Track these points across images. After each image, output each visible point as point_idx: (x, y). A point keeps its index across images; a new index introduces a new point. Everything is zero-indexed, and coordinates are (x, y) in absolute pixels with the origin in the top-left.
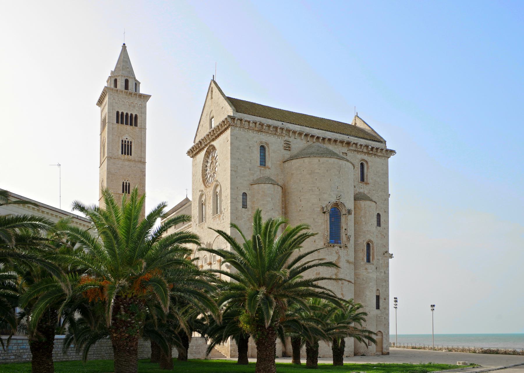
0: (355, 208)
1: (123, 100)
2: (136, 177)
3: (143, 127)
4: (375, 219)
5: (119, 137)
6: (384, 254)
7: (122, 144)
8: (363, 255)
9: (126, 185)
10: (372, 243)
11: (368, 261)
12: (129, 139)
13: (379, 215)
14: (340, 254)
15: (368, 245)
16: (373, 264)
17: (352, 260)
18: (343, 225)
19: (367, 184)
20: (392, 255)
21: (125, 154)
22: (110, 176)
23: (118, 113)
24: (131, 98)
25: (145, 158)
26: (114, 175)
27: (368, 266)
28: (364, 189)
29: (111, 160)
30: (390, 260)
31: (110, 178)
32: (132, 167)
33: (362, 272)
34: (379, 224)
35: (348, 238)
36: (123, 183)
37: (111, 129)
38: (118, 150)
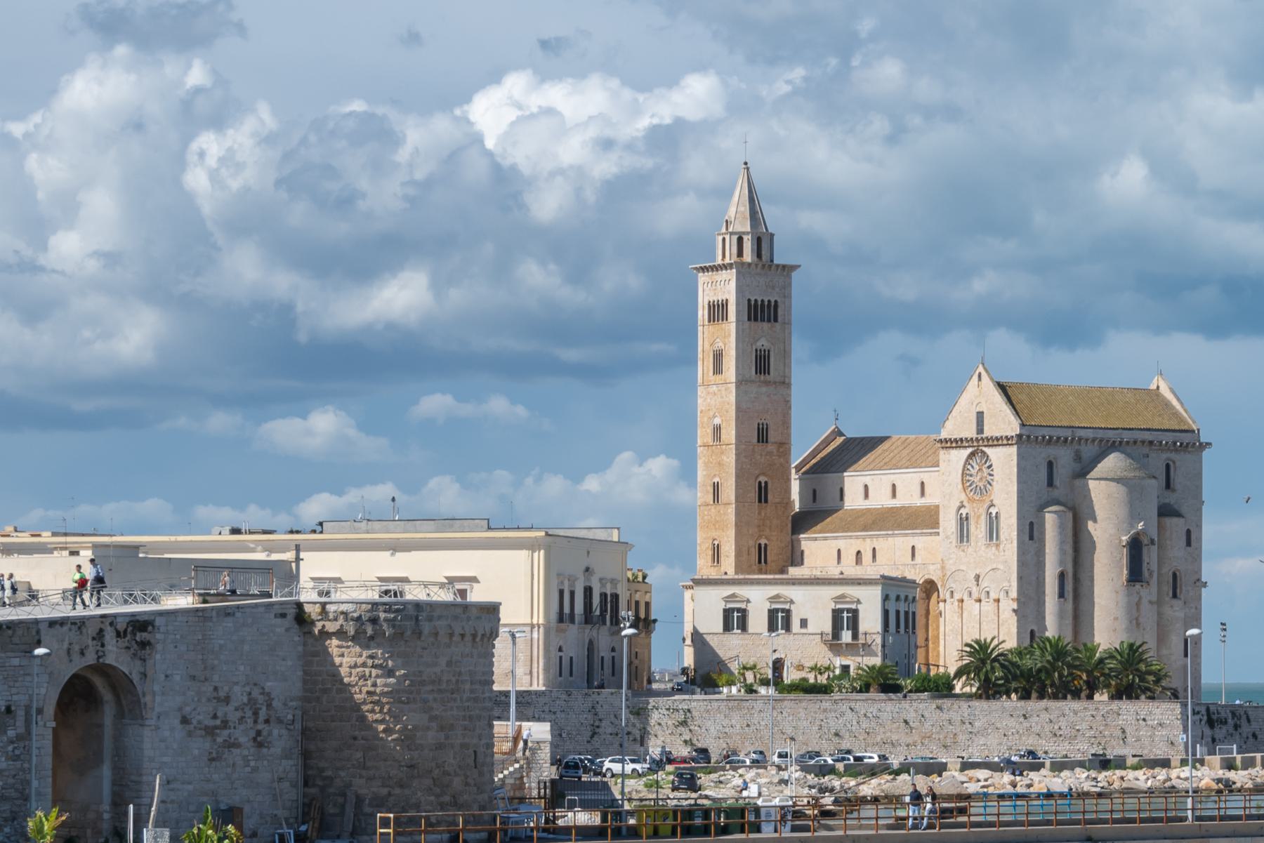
0: (1159, 535)
3: (786, 321)
4: (1184, 538)
5: (752, 345)
6: (1195, 583)
8: (1168, 589)
9: (763, 429)
10: (1180, 573)
11: (1175, 596)
13: (1189, 532)
14: (1141, 593)
15: (1175, 575)
16: (1180, 599)
17: (1155, 599)
18: (1145, 559)
19: (1174, 491)
20: (1206, 583)
21: (761, 373)
25: (790, 378)
27: (1175, 602)
28: (1171, 499)
30: (1203, 589)
33: (1167, 611)
34: (1189, 543)
35: (1151, 574)
36: (759, 424)
37: (741, 333)
38: (750, 368)
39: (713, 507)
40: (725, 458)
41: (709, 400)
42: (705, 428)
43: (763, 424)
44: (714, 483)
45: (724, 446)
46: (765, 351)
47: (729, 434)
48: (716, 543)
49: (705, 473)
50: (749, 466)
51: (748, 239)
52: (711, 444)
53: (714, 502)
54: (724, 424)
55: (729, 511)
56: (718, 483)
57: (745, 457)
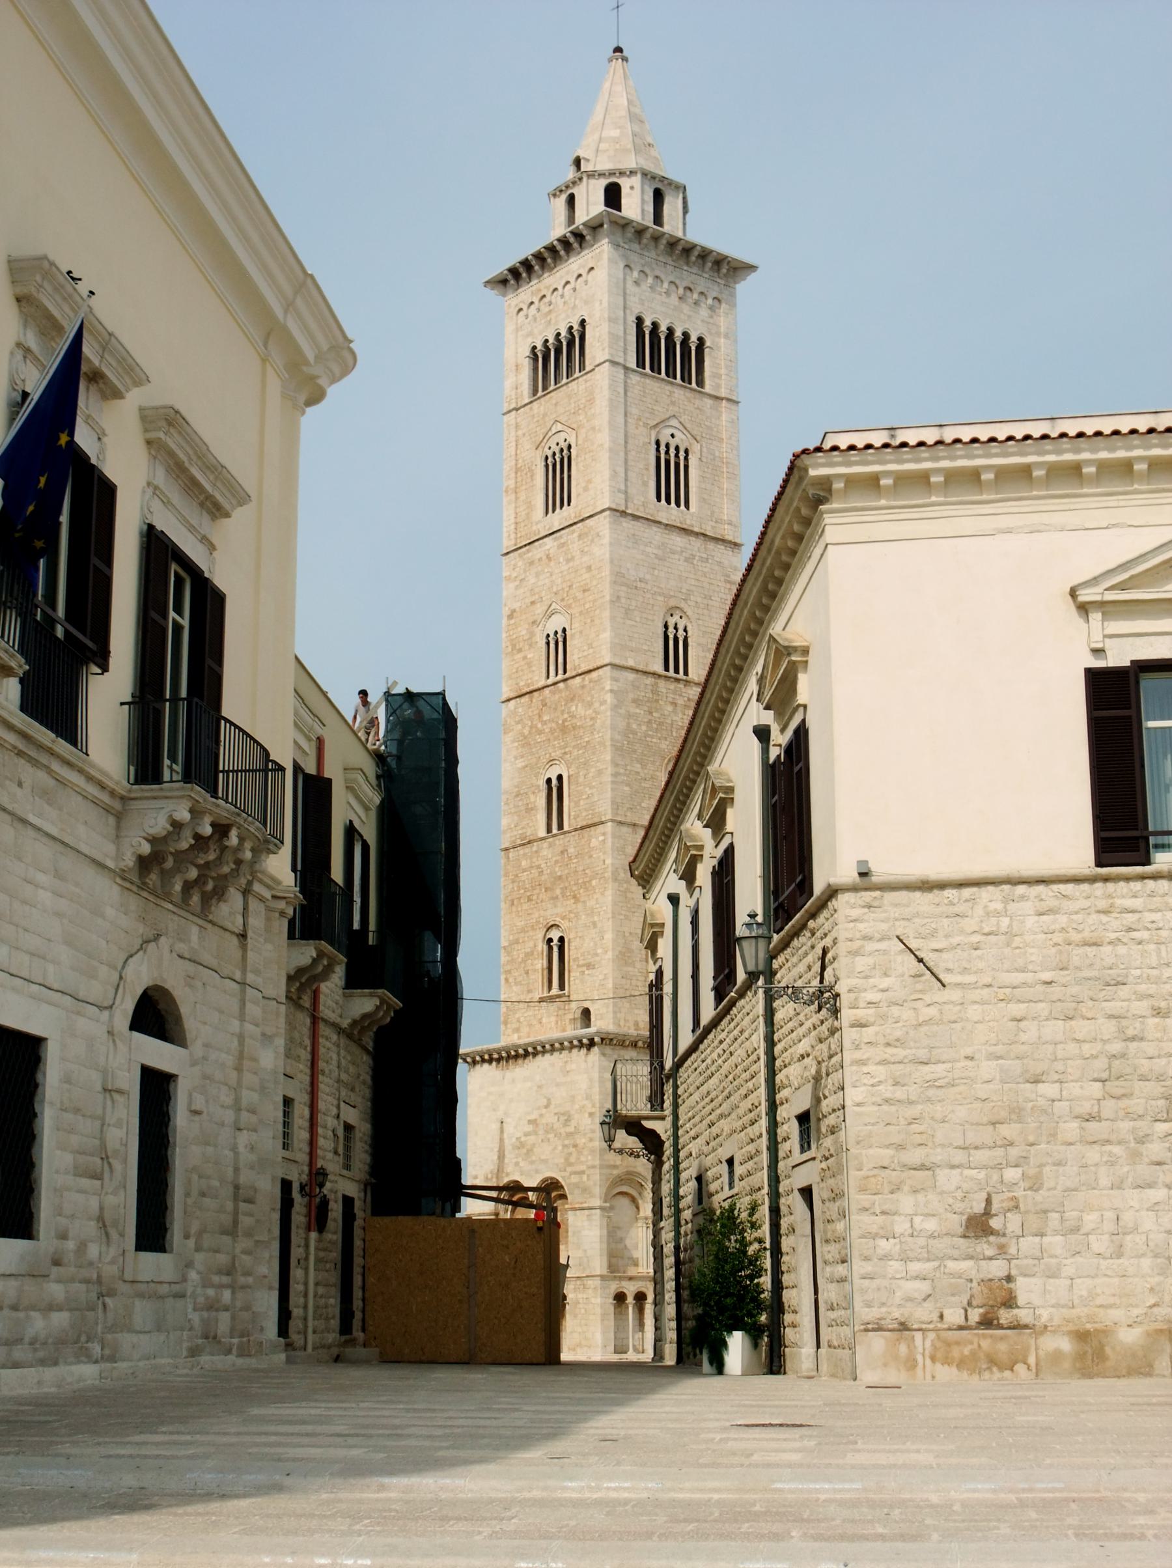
1: (657, 273)
2: (710, 602)
7: (658, 459)
12: (681, 440)
21: (668, 501)
22: (622, 594)
23: (640, 321)
24: (685, 268)
26: (636, 588)
29: (625, 524)
31: (623, 600)
32: (697, 558)
36: (666, 626)
38: (645, 484)
39: (545, 844)
40: (578, 709)
41: (533, 580)
42: (520, 650)
43: (676, 628)
44: (549, 781)
45: (578, 679)
46: (677, 448)
47: (590, 646)
48: (555, 935)
49: (520, 763)
50: (644, 728)
51: (632, 188)
52: (542, 683)
53: (549, 830)
54: (576, 625)
55: (594, 842)
56: (560, 778)
57: (635, 701)
